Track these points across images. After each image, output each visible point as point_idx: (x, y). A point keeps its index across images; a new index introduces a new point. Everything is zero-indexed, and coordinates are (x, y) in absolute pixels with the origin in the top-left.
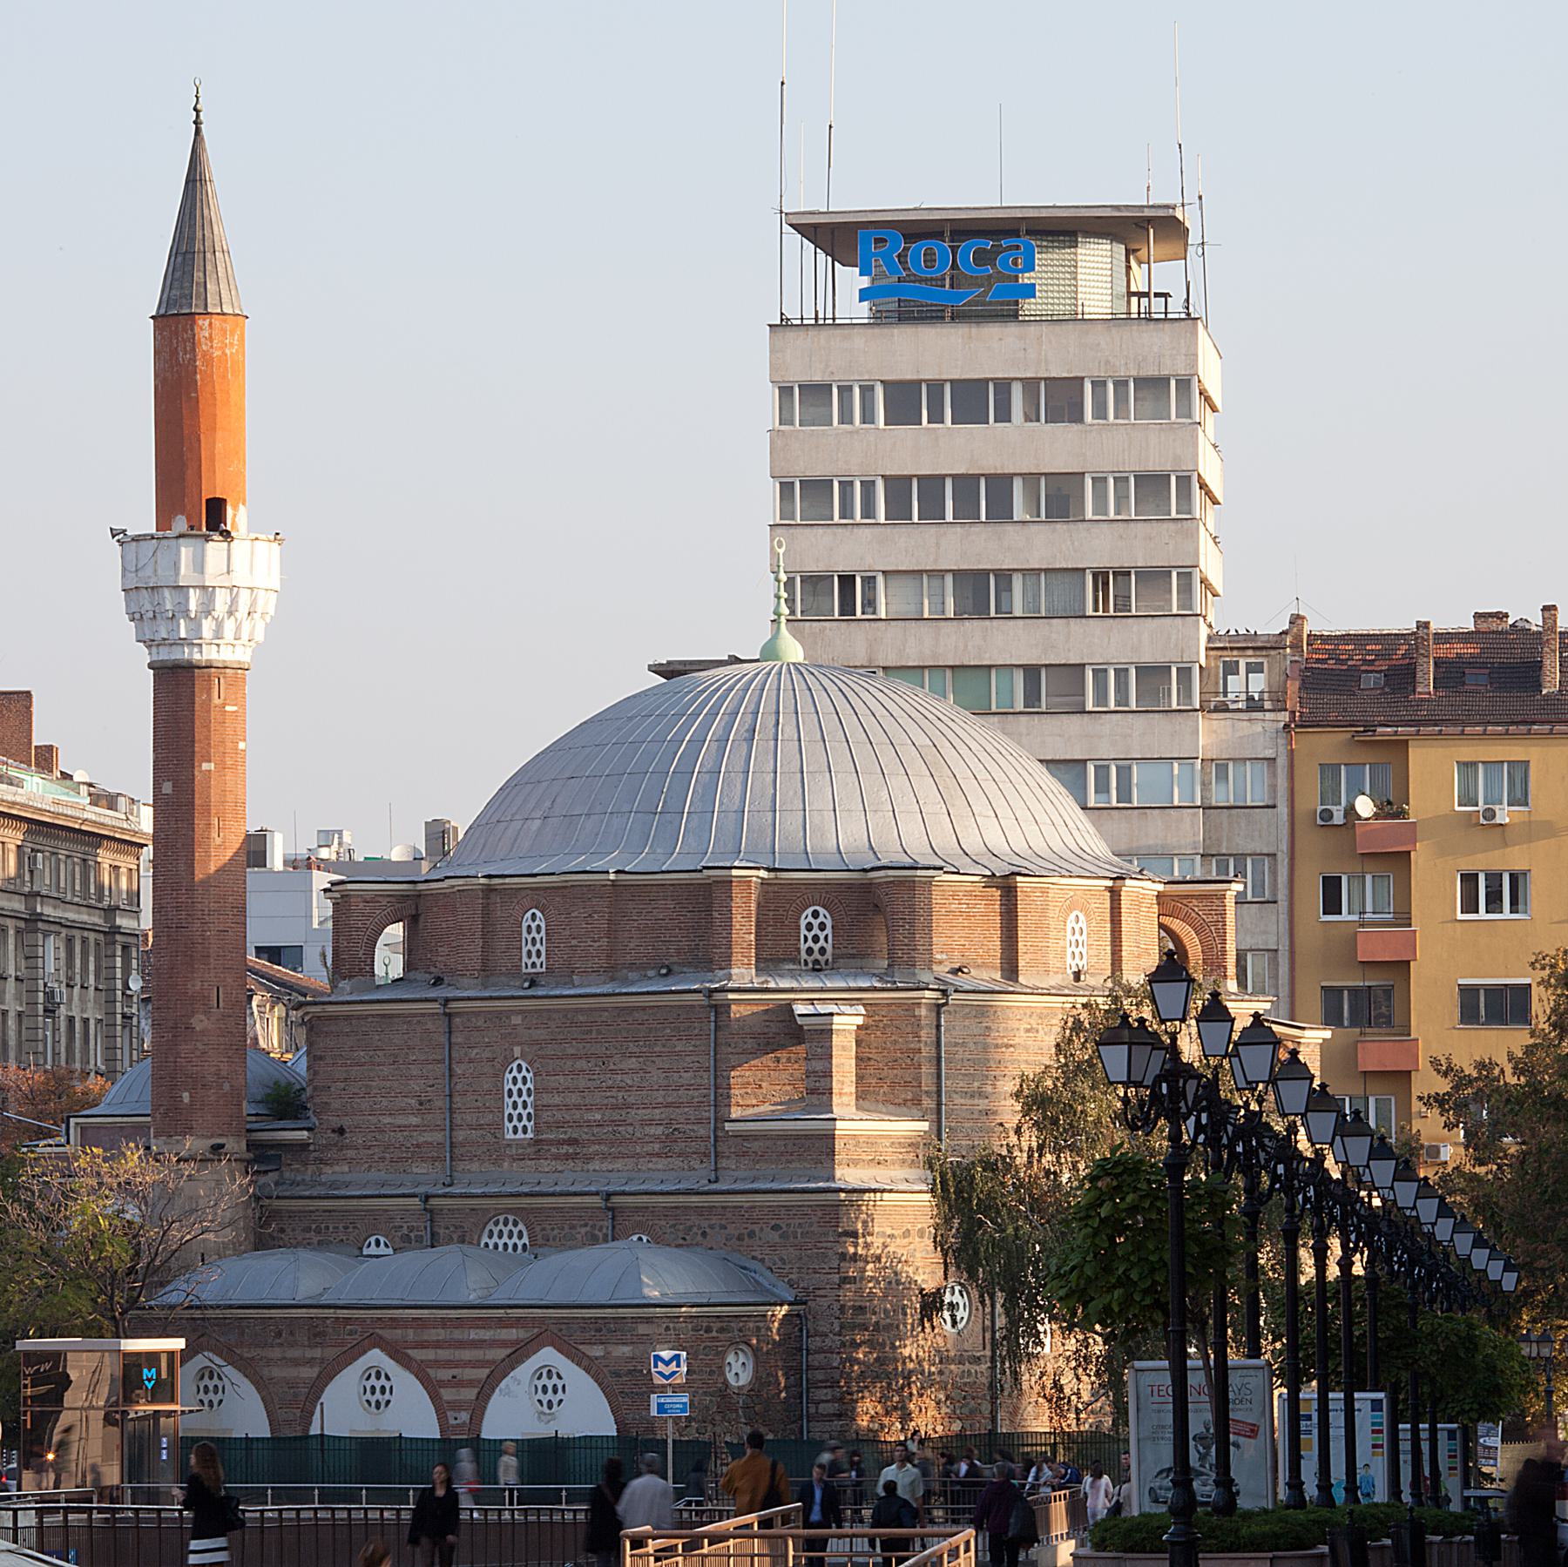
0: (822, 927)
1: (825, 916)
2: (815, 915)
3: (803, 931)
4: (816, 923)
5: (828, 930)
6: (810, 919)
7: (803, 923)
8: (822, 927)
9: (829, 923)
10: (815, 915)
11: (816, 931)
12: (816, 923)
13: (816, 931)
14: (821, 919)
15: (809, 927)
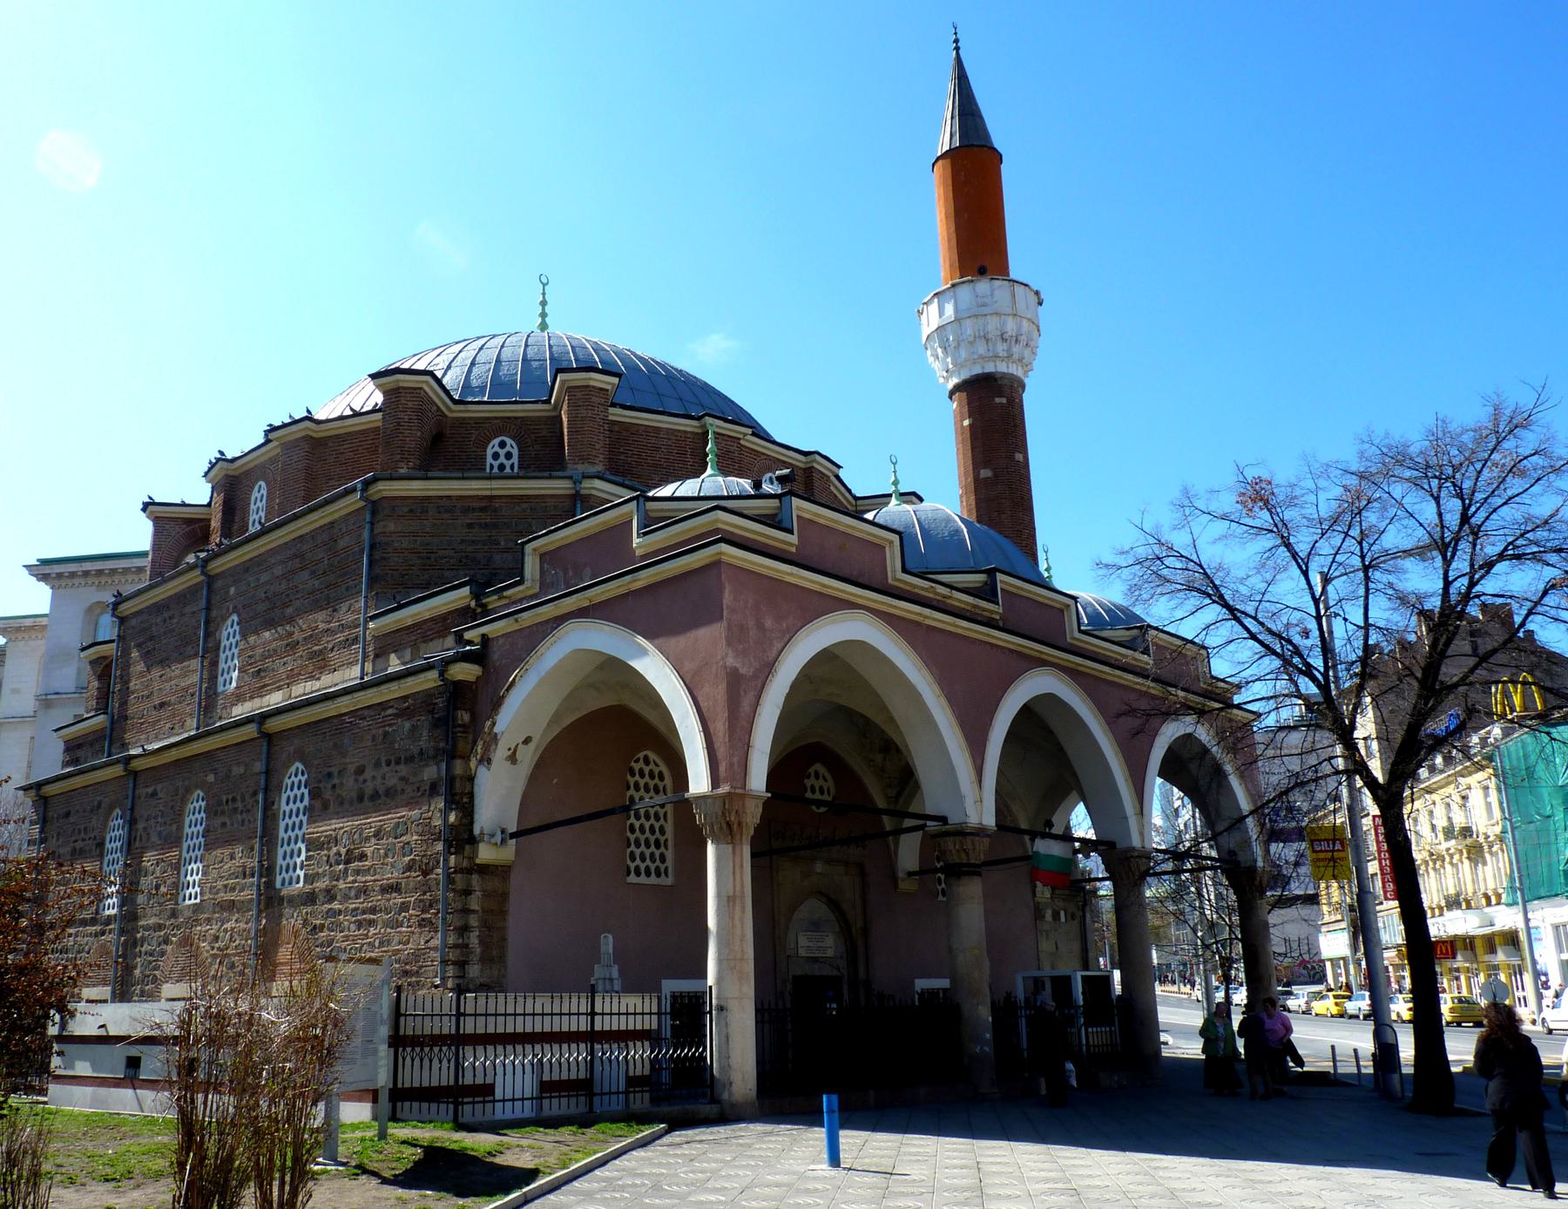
0: (509, 456)
1: (512, 446)
2: (502, 445)
3: (489, 460)
4: (502, 452)
5: (515, 460)
6: (497, 449)
7: (489, 452)
8: (509, 456)
9: (515, 452)
10: (502, 445)
11: (502, 459)
12: (502, 452)
13: (502, 459)
14: (508, 448)
15: (496, 456)
